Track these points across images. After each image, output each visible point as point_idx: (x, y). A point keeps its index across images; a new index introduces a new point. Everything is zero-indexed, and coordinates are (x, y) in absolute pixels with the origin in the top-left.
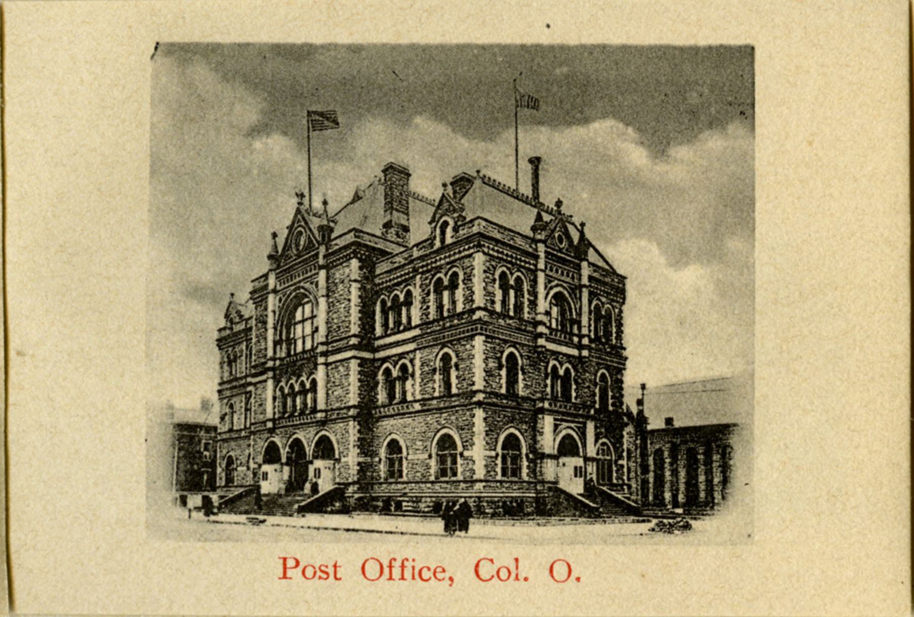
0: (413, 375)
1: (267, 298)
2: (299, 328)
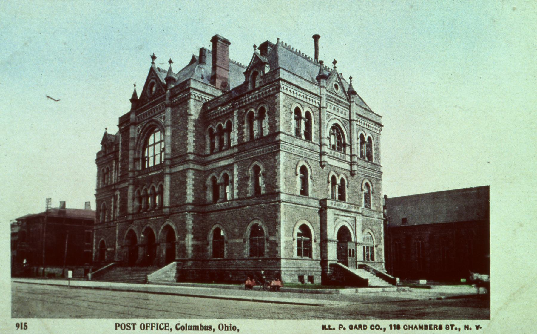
0: (232, 182)
1: (129, 129)
2: (151, 149)
